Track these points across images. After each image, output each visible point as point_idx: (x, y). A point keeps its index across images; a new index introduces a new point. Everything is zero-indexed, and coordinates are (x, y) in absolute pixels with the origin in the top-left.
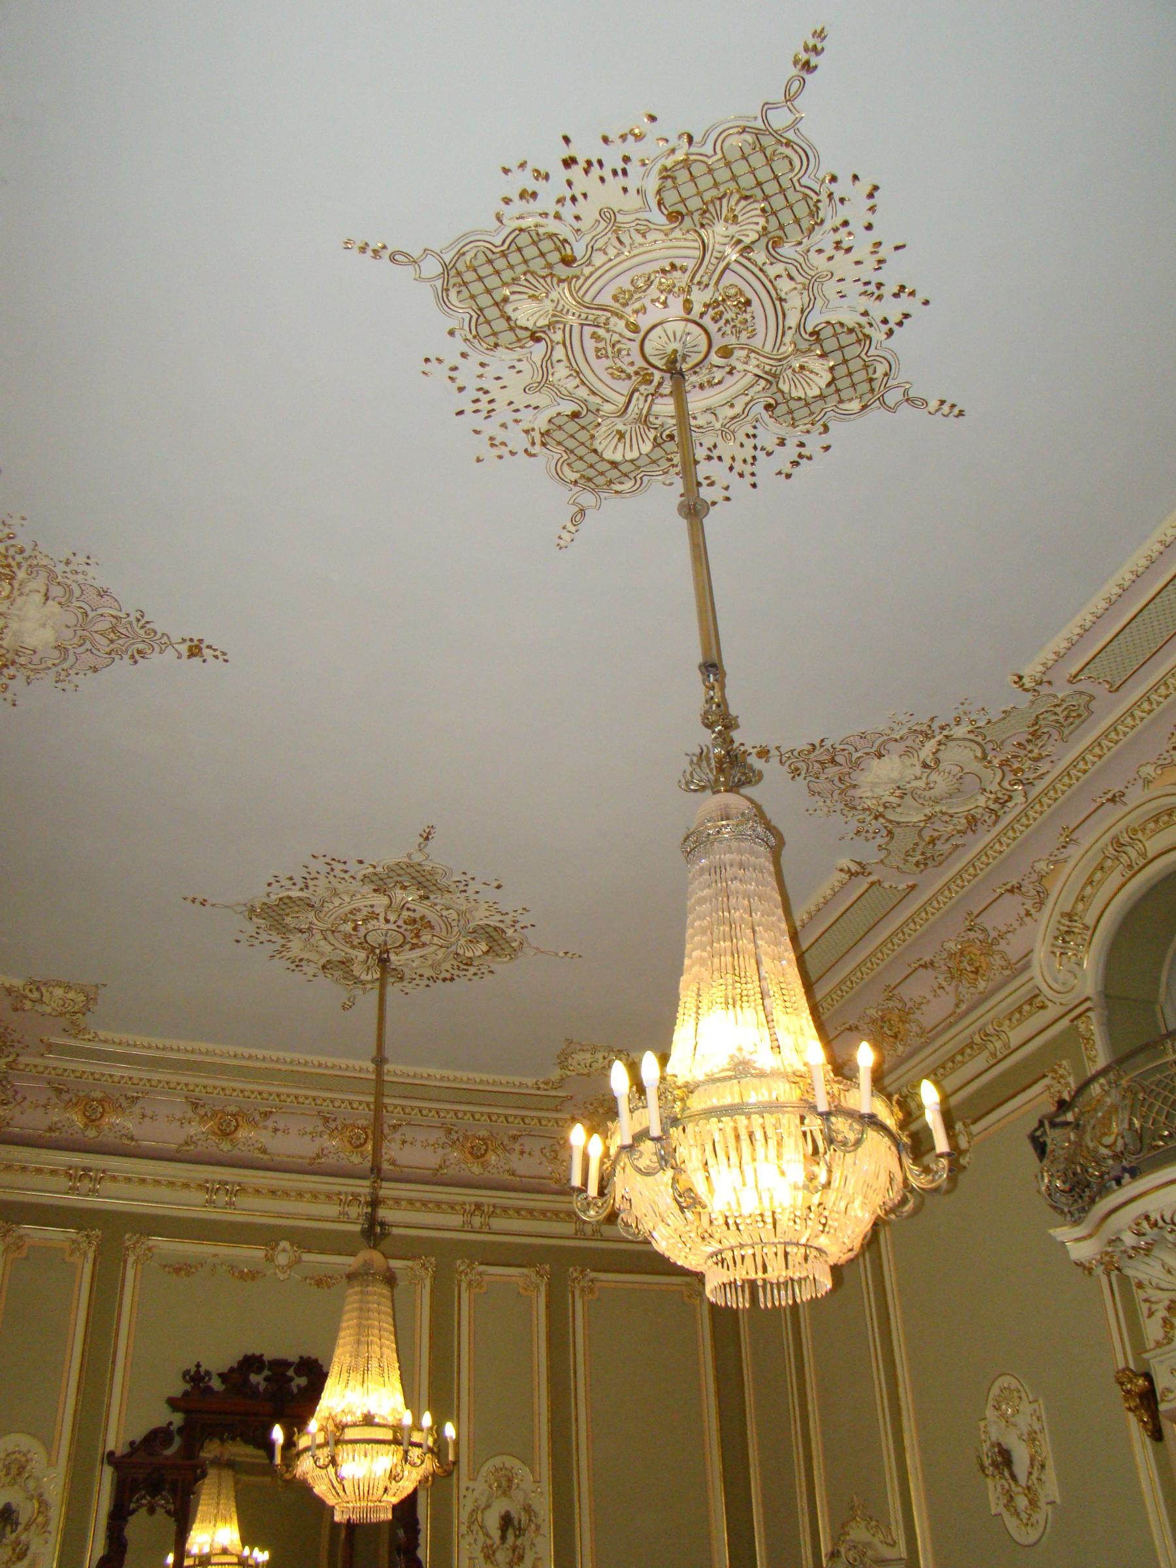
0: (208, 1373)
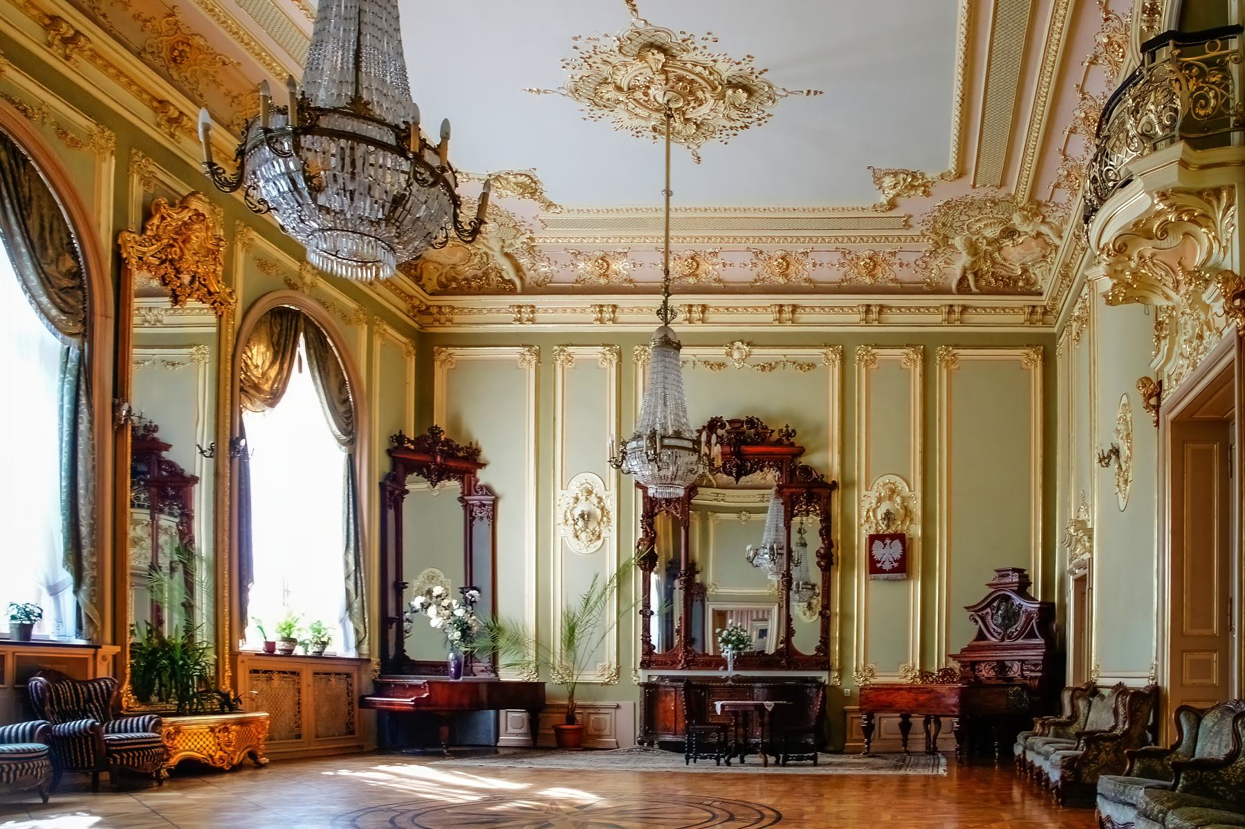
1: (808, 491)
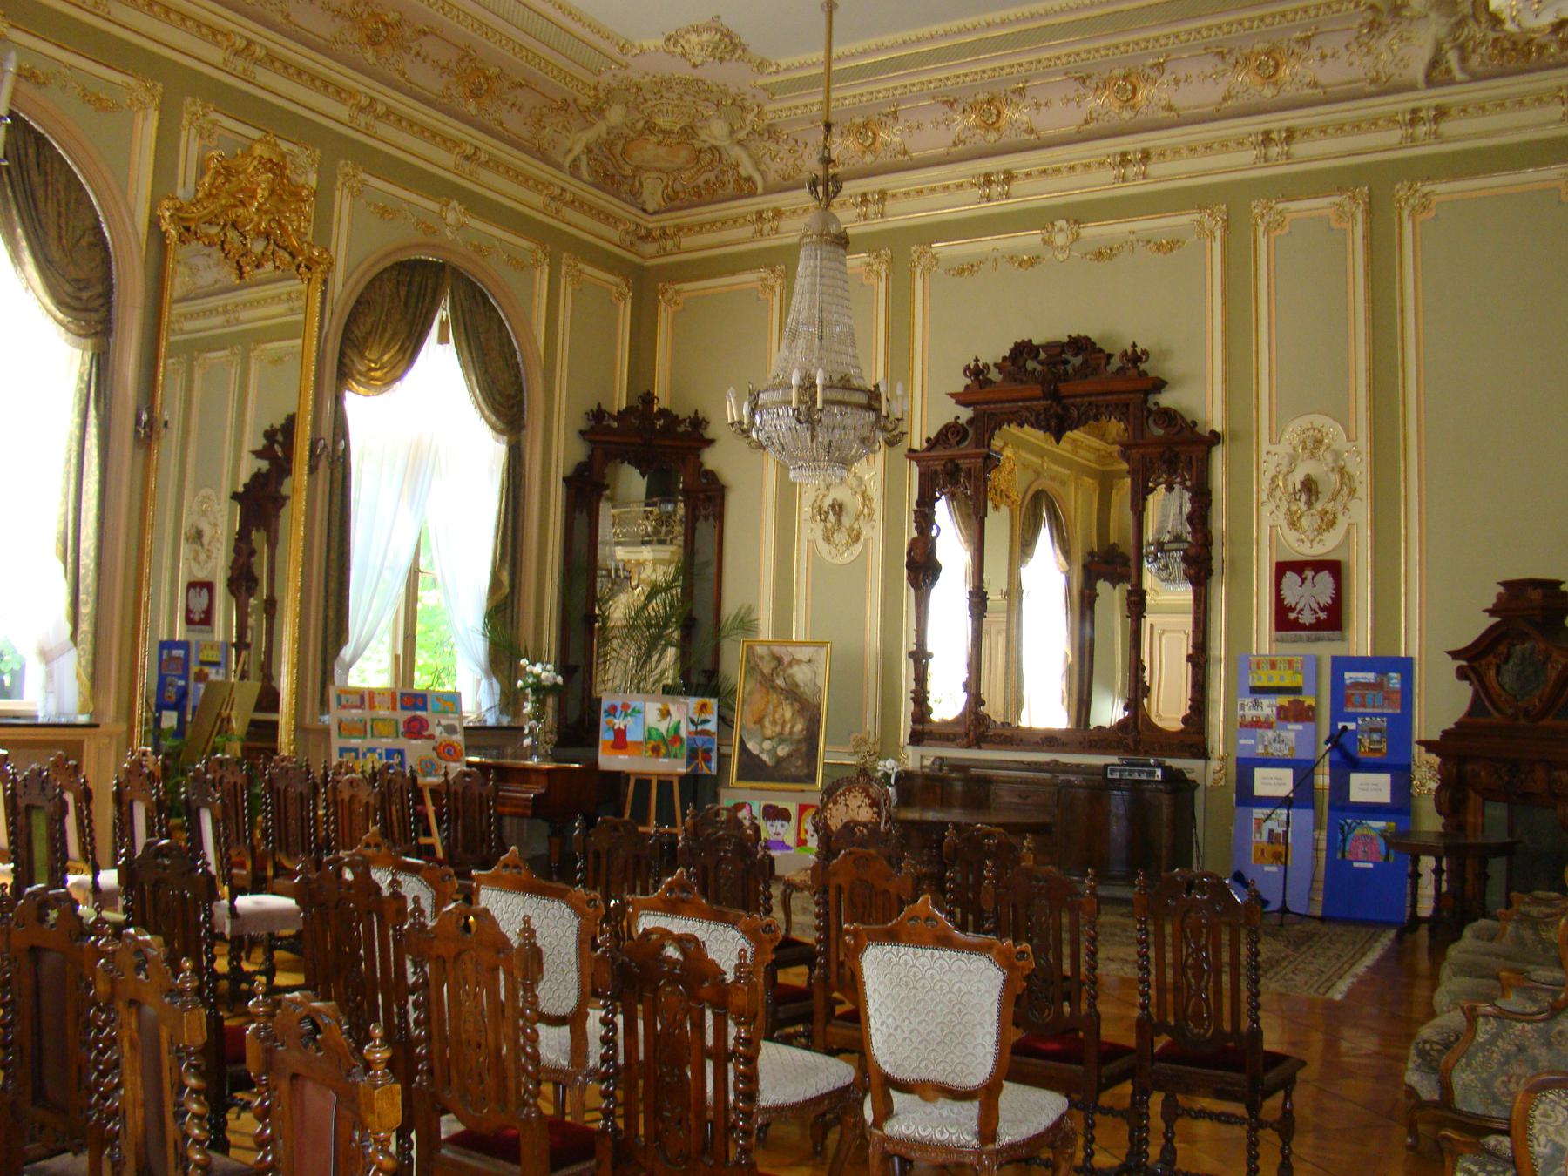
0: (986, 366)
1: (1175, 450)
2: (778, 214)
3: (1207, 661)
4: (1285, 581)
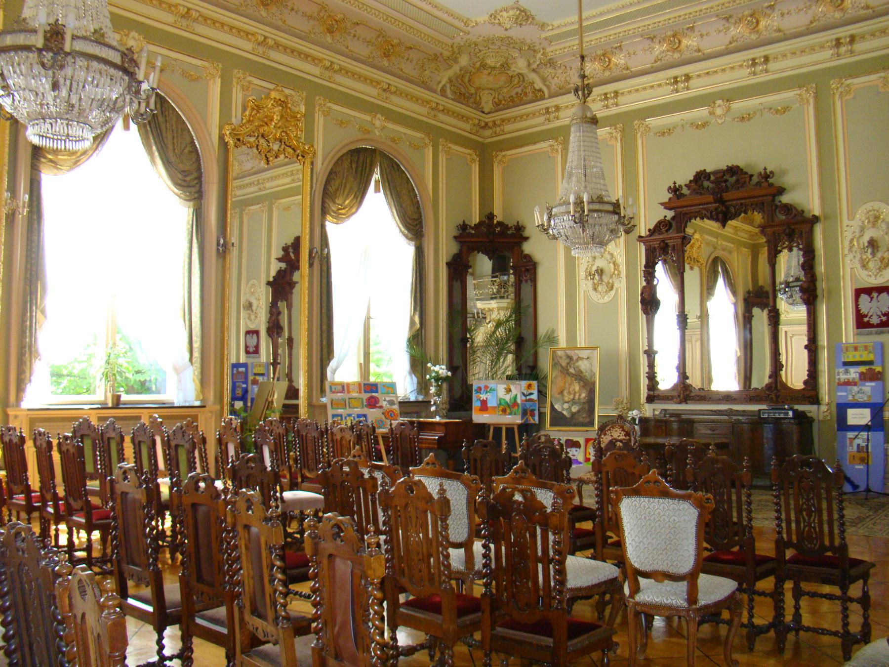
0: (680, 186)
1: (791, 227)
2: (558, 108)
3: (816, 348)
4: (860, 300)
